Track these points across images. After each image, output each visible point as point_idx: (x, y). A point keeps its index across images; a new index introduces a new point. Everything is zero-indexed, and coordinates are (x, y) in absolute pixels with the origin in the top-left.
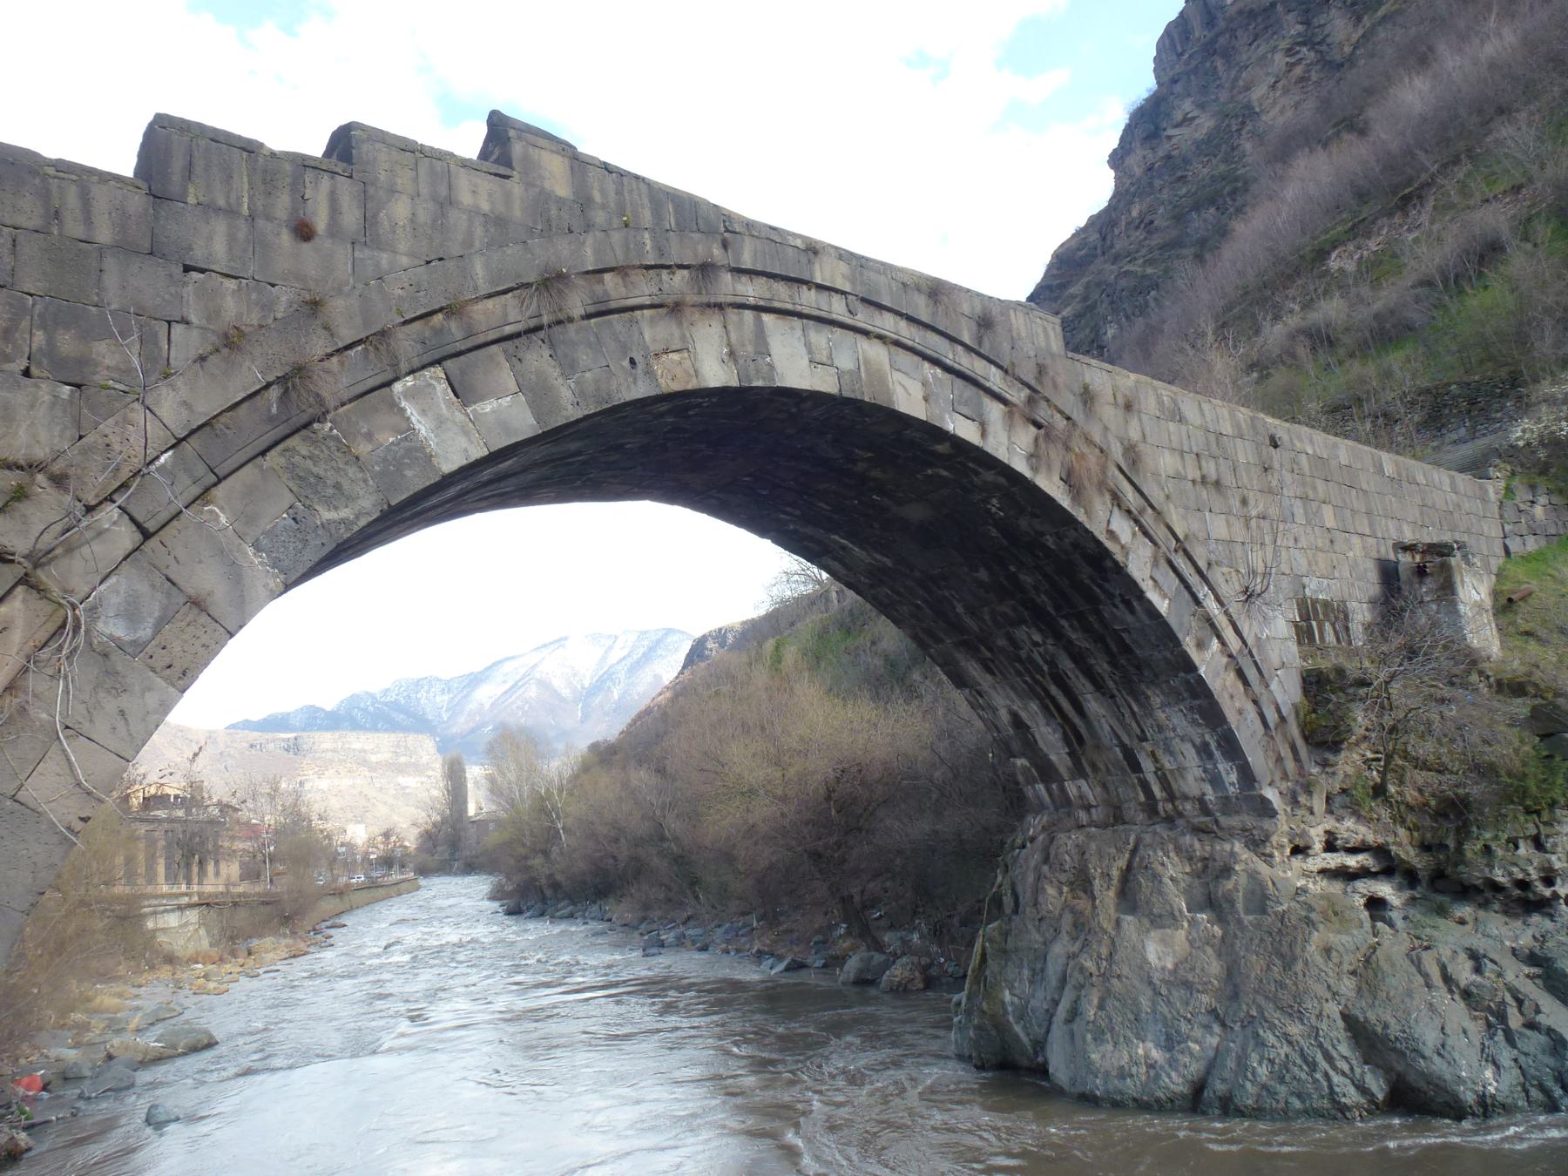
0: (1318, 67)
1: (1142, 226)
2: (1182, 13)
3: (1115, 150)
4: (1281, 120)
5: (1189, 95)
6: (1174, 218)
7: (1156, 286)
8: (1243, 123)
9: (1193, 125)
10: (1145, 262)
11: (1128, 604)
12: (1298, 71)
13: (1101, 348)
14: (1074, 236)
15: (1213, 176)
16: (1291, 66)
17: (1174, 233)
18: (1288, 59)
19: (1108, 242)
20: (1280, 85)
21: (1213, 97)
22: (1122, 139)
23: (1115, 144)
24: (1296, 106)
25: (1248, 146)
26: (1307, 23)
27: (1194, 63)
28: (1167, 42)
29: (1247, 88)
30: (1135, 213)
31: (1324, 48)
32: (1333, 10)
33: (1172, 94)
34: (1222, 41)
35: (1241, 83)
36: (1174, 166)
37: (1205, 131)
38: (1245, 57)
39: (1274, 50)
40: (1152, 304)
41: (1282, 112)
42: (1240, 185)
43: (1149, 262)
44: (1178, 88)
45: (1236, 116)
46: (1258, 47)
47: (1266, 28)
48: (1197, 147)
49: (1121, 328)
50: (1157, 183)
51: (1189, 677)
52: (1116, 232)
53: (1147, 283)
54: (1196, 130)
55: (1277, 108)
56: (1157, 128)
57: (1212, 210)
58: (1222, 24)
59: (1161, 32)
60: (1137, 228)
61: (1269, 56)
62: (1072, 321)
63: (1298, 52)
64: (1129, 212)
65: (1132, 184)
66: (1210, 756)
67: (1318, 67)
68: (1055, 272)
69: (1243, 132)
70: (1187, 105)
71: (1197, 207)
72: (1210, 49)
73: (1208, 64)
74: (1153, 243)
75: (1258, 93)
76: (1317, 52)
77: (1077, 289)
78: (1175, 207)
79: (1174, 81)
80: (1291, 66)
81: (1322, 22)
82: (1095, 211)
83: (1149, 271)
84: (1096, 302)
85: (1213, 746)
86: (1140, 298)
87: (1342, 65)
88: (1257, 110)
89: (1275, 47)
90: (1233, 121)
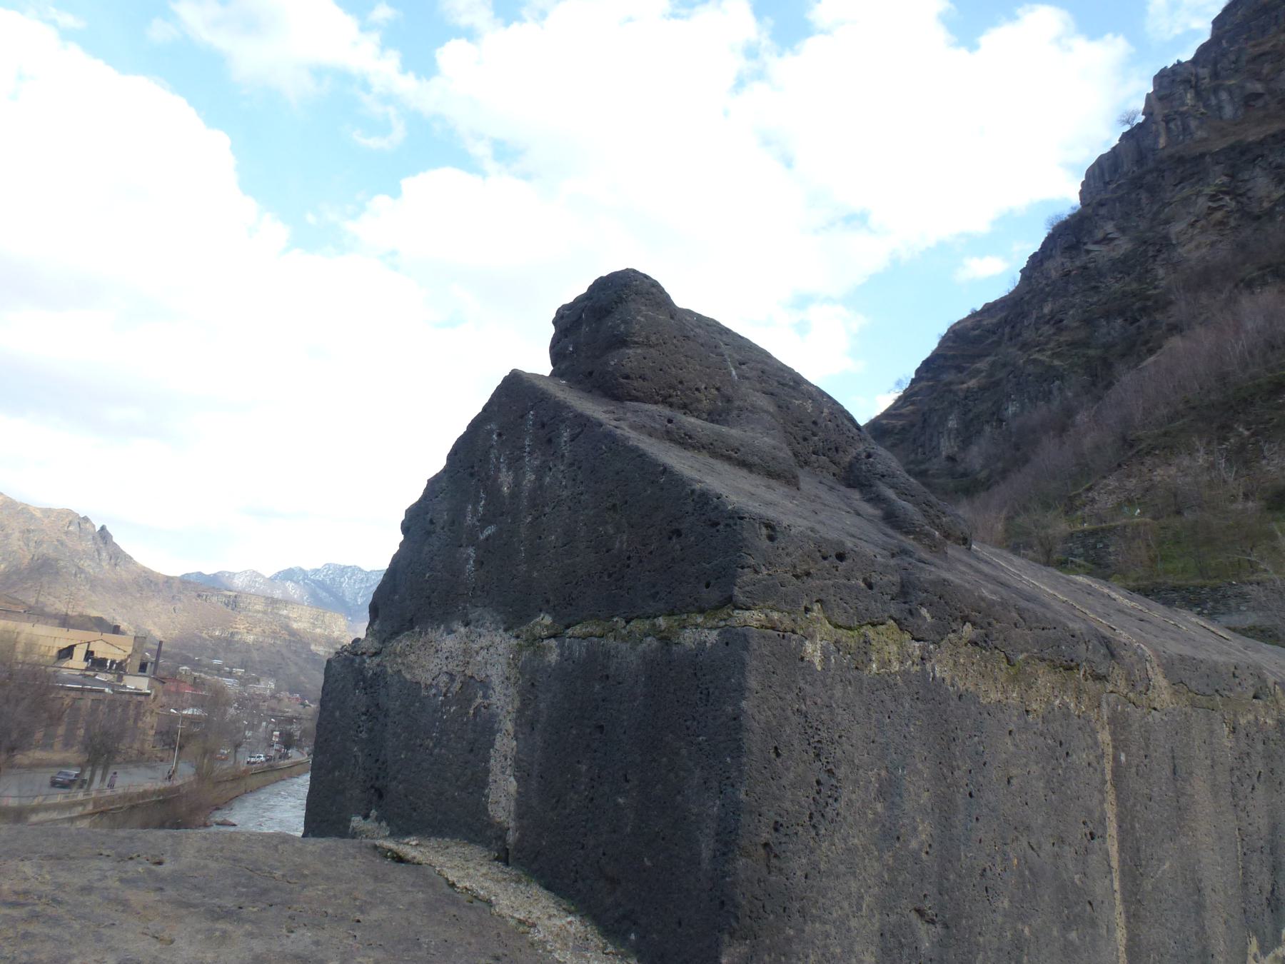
0: (1237, 215)
1: (1052, 322)
2: (1114, 149)
3: (1035, 254)
4: (1196, 255)
5: (1112, 219)
6: (1085, 321)
7: (1062, 378)
8: (1159, 251)
9: (1112, 245)
10: (1053, 354)
12: (1219, 215)
13: (1001, 421)
14: (969, 317)
15: (1123, 292)
16: (1212, 210)
17: (1082, 334)
18: (1210, 204)
19: (1017, 331)
20: (1199, 225)
21: (1134, 224)
22: (1044, 245)
23: (1035, 247)
24: (1213, 244)
25: (1161, 272)
26: (1232, 176)
27: (1120, 193)
28: (1097, 171)
29: (1167, 222)
30: (1046, 310)
31: (1244, 200)
32: (1258, 170)
33: (1097, 215)
34: (1149, 178)
35: (1162, 216)
36: (1089, 277)
37: (1122, 252)
38: (1169, 195)
39: (1198, 194)
40: (1056, 392)
41: (1198, 247)
42: (1149, 303)
43: (1055, 355)
44: (1103, 211)
45: (1154, 244)
46: (1183, 188)
47: (1192, 175)
48: (1113, 264)
49: (1023, 407)
50: (1072, 288)
52: (1026, 323)
54: (1113, 250)
55: (1194, 244)
56: (1078, 242)
57: (1120, 321)
58: (1151, 164)
60: (1048, 322)
61: (1194, 198)
62: (976, 392)
63: (1221, 199)
64: (1041, 308)
65: (1047, 285)
67: (1237, 215)
68: (950, 344)
69: (1158, 259)
70: (1109, 227)
71: (1107, 316)
72: (1137, 183)
73: (1133, 196)
74: (1062, 339)
75: (1176, 228)
76: (1238, 202)
77: (982, 365)
78: (1085, 312)
79: (1101, 204)
80: (1212, 210)
81: (1246, 177)
82: (991, 300)
83: (1056, 363)
84: (1001, 380)
86: (1045, 385)
87: (1258, 218)
88: (1174, 242)
89: (1200, 191)
90: (1151, 248)
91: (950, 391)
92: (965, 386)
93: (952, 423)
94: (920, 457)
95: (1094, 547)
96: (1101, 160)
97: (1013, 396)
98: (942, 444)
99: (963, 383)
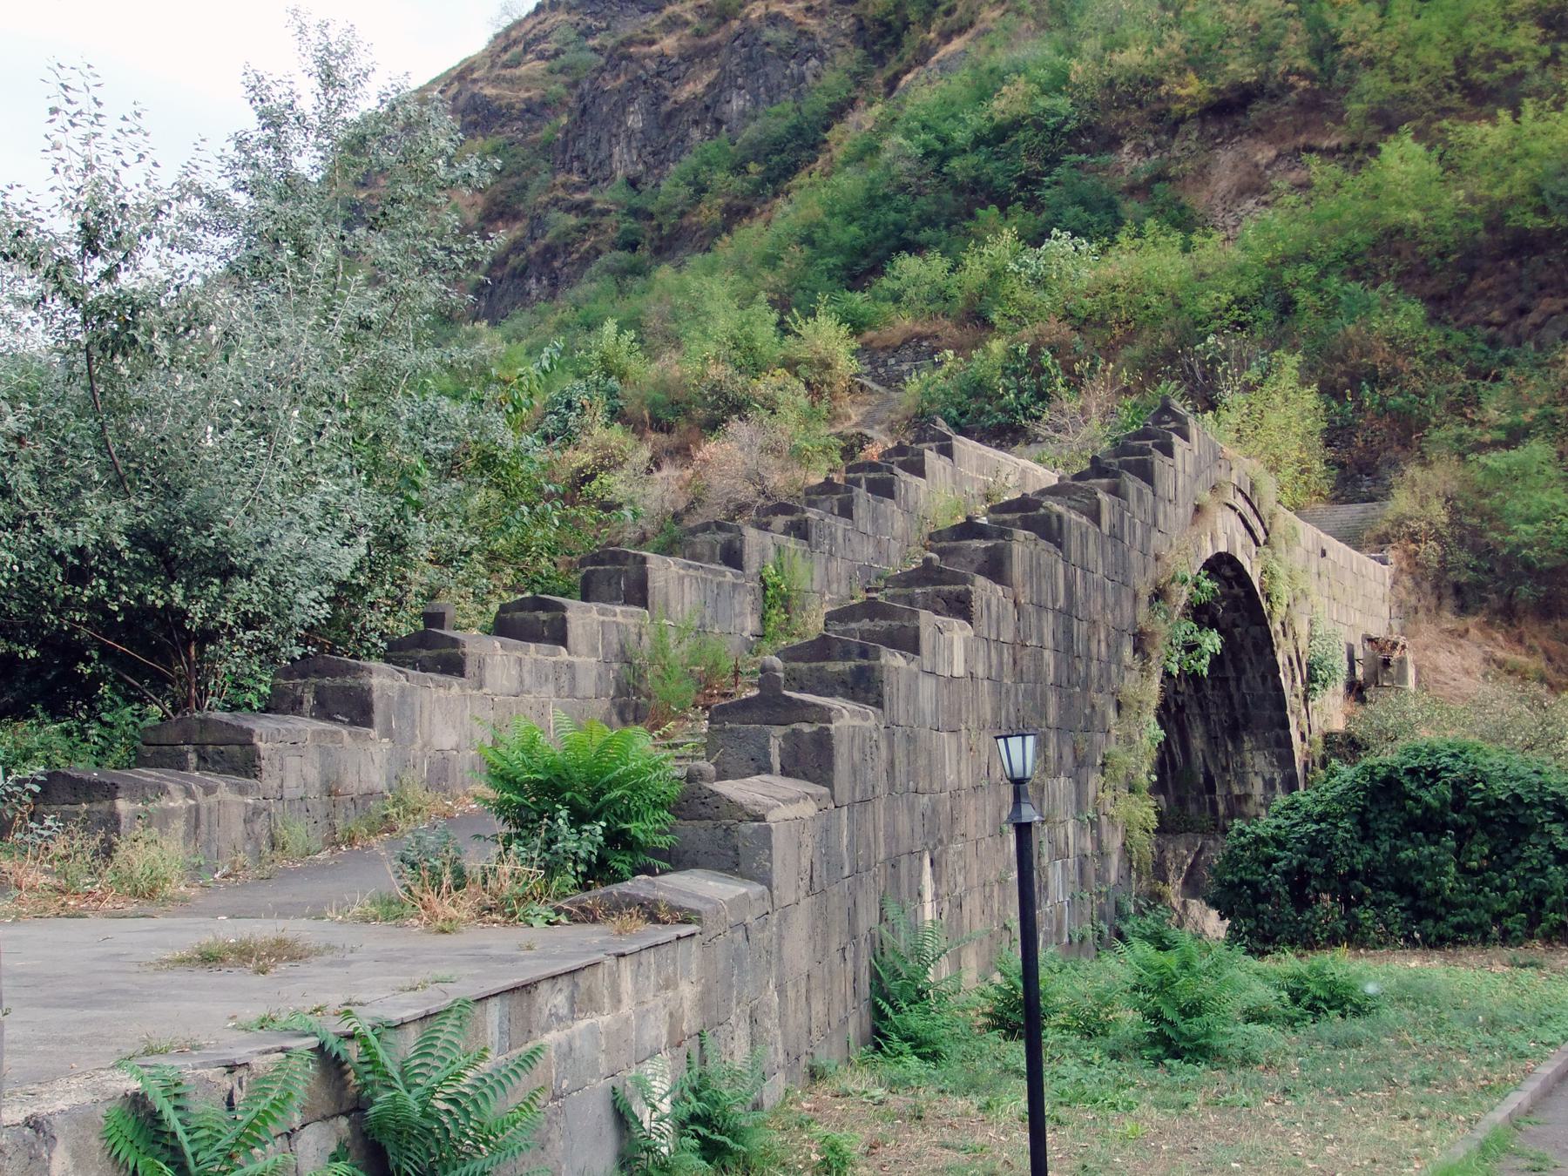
7: (822, 58)
11: (1264, 678)
13: (719, 123)
49: (756, 102)
51: (1281, 732)
53: (805, 44)
66: (1273, 788)
83: (812, 23)
85: (1278, 781)
86: (792, 64)
91: (629, 58)
92: (655, 48)
93: (635, 121)
94: (576, 178)
95: (885, 364)
97: (740, 81)
98: (616, 157)
99: (652, 43)
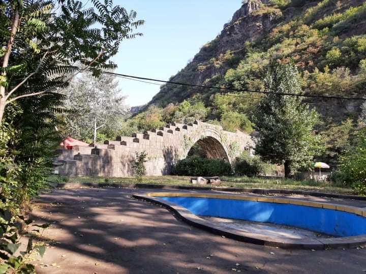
12: (259, 31)
30: (223, 50)
59: (235, 11)
75: (251, 32)
93: (200, 78)
96: (238, 11)
